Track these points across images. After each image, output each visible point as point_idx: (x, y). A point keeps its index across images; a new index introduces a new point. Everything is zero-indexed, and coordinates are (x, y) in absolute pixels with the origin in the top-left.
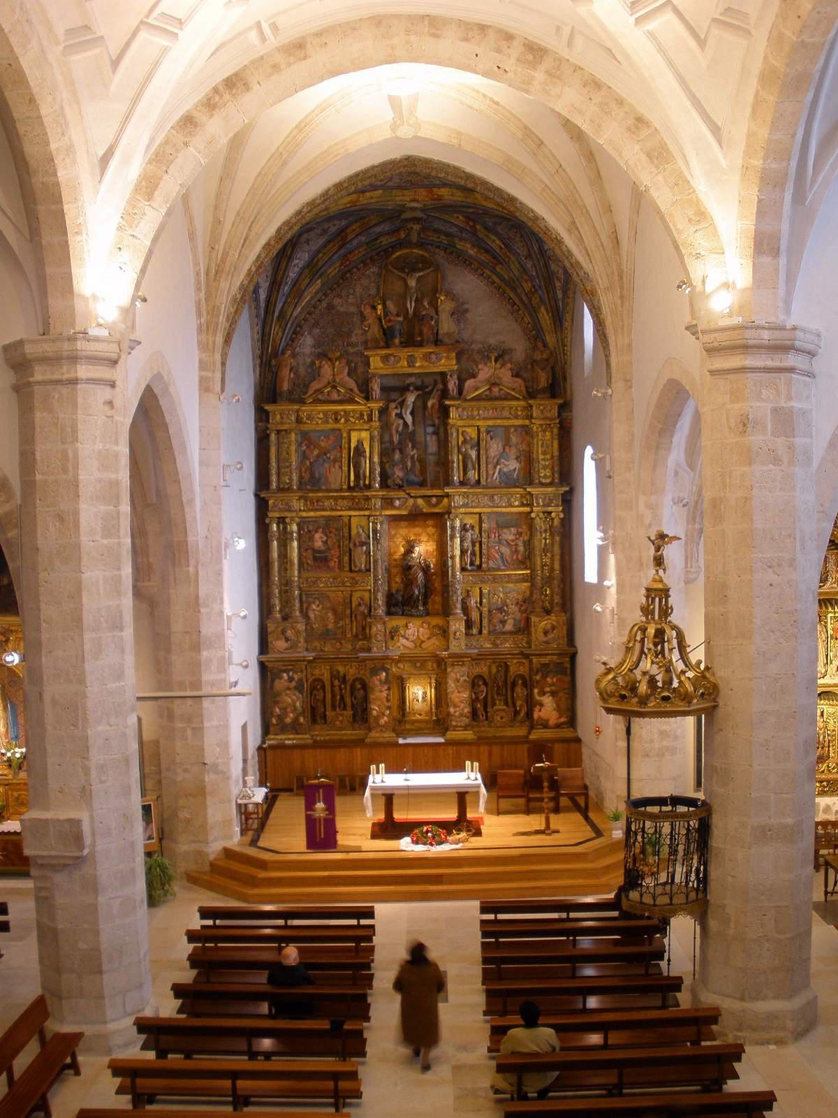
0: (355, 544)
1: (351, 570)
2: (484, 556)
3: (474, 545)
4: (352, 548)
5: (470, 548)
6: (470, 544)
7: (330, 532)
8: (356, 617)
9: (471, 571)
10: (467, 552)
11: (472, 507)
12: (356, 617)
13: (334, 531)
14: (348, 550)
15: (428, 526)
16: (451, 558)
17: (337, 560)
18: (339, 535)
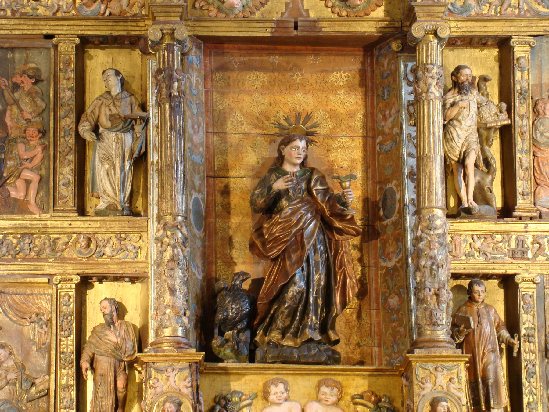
0: (96, 129)
1: (82, 211)
2: (520, 173)
3: (484, 141)
4: (88, 136)
5: (476, 146)
6: (475, 137)
7: (16, 87)
8: (92, 362)
9: (481, 218)
10: (462, 162)
11: (479, 18)
12: (92, 362)
13: (28, 84)
14: (71, 141)
15: (335, 89)
16: (412, 175)
17: (34, 177)
18: (44, 97)
